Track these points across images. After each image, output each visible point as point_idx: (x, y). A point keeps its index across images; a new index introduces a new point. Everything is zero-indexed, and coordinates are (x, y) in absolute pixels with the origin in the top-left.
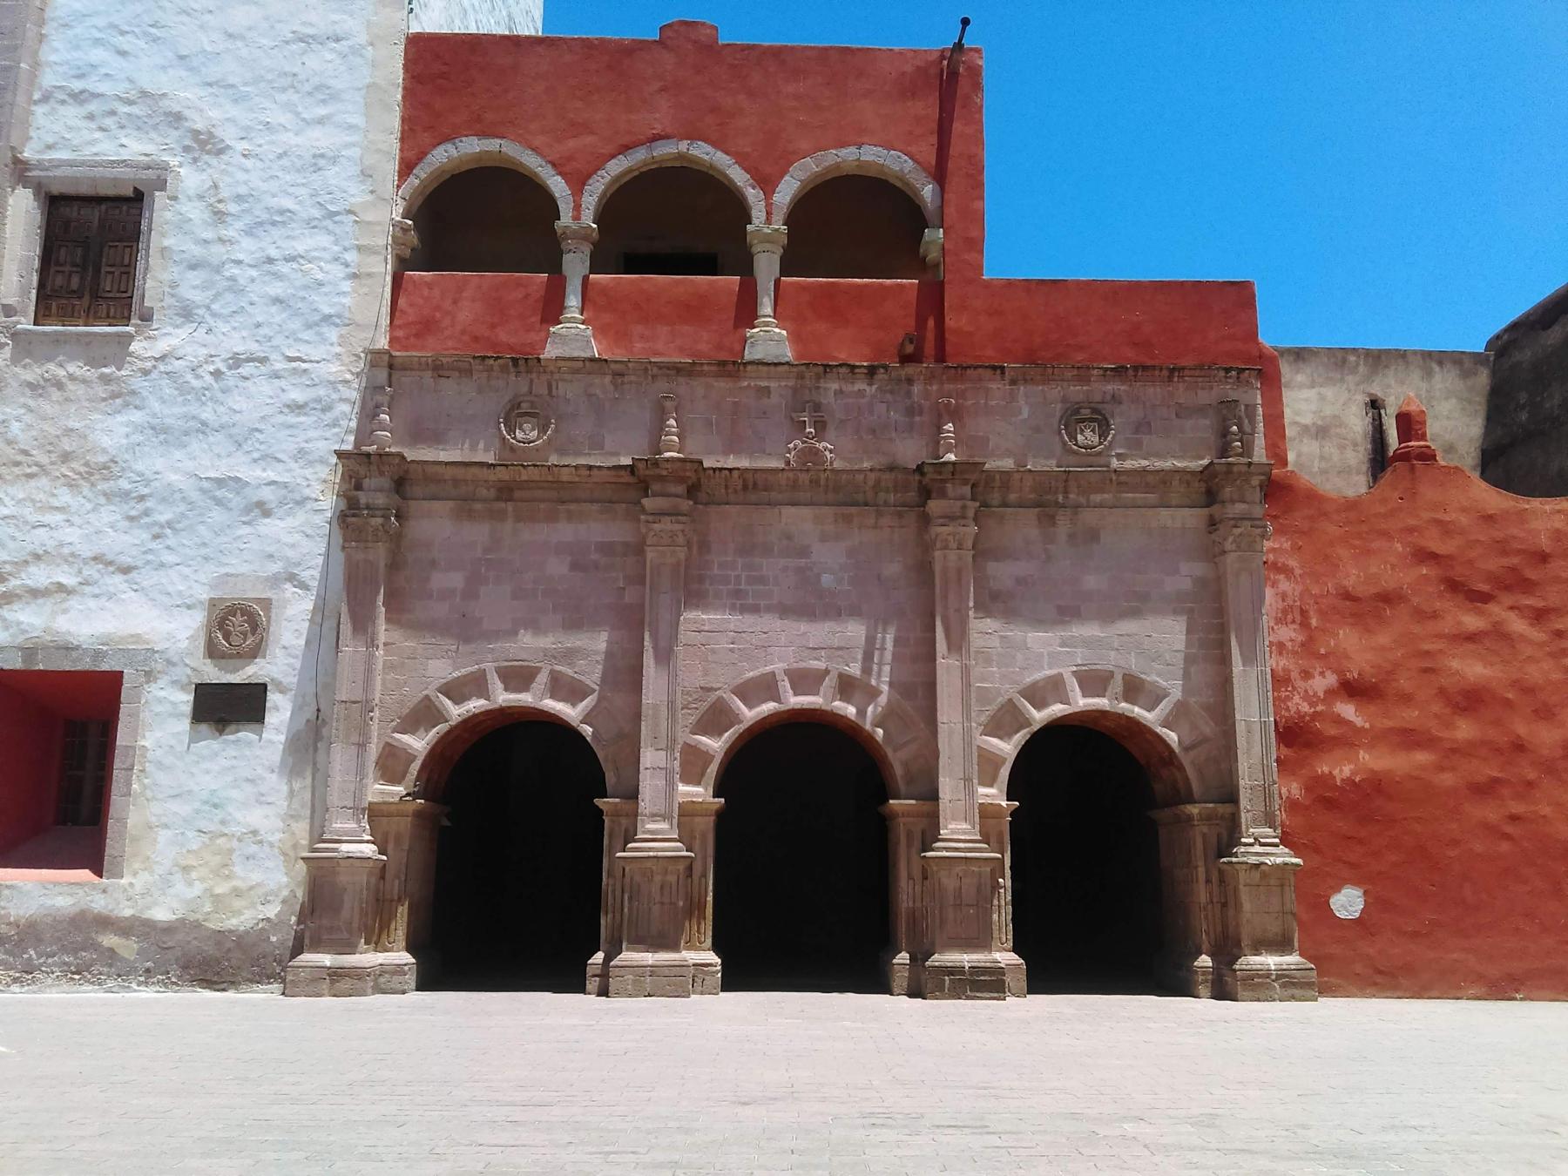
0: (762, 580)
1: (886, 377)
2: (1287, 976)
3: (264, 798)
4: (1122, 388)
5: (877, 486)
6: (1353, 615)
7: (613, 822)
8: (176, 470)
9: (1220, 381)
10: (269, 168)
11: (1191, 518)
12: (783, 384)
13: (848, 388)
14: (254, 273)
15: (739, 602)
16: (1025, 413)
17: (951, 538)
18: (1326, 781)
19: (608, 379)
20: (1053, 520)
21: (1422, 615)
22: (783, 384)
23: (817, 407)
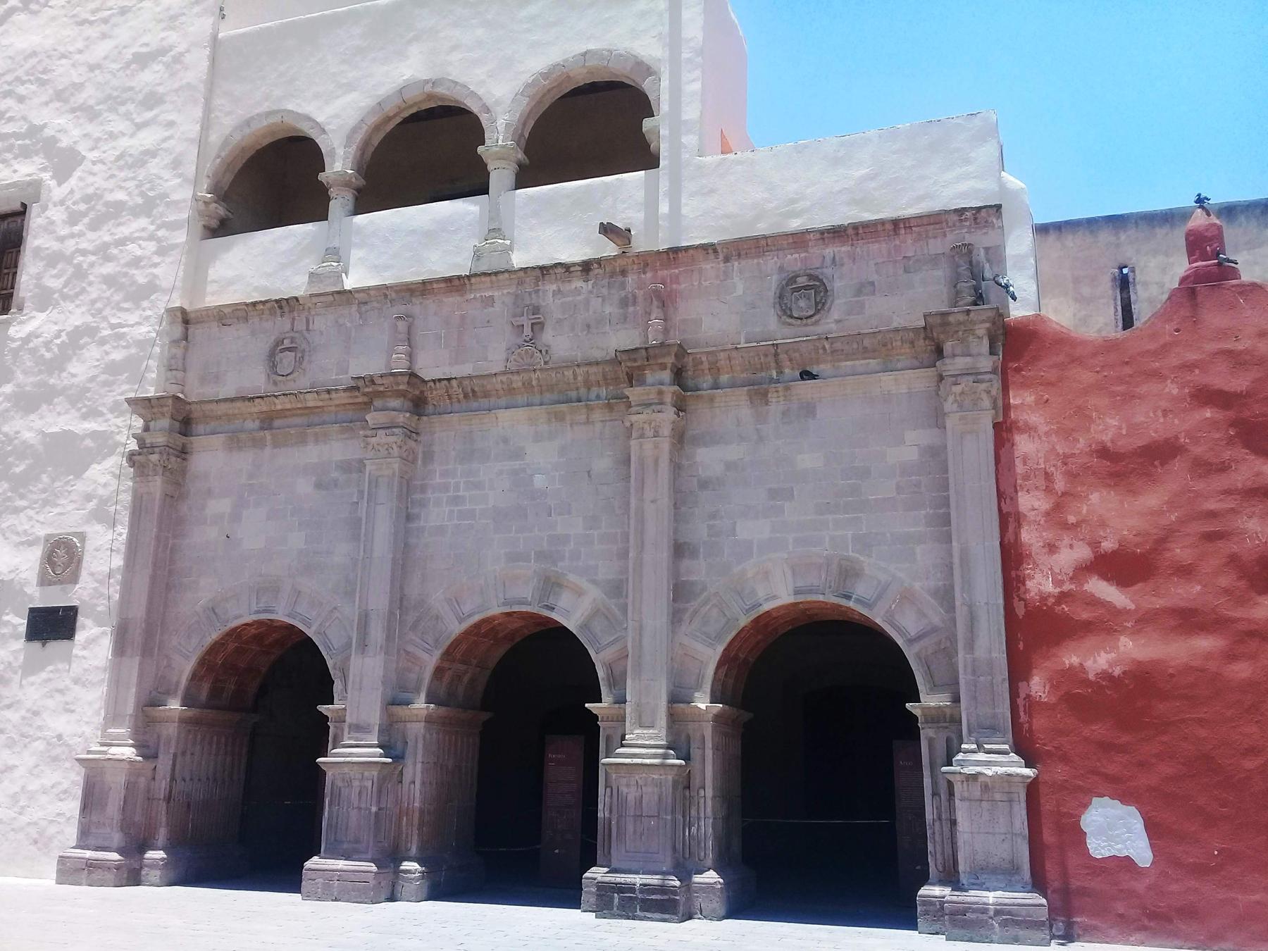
0: (478, 486)
1: (601, 271)
2: (1009, 913)
3: (68, 707)
4: (843, 249)
5: (588, 385)
6: (1113, 475)
7: (335, 727)
8: (31, 429)
9: (954, 226)
10: (110, 169)
11: (920, 380)
12: (505, 291)
13: (567, 287)
14: (93, 258)
15: (456, 509)
16: (740, 290)
17: (646, 426)
18: (1074, 675)
19: (354, 308)
20: (764, 395)
21: (1204, 468)
22: (505, 291)
23: (536, 310)
